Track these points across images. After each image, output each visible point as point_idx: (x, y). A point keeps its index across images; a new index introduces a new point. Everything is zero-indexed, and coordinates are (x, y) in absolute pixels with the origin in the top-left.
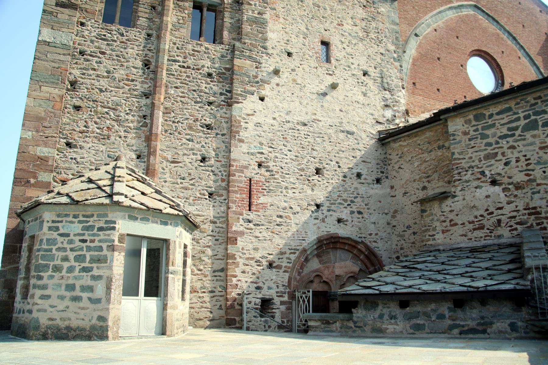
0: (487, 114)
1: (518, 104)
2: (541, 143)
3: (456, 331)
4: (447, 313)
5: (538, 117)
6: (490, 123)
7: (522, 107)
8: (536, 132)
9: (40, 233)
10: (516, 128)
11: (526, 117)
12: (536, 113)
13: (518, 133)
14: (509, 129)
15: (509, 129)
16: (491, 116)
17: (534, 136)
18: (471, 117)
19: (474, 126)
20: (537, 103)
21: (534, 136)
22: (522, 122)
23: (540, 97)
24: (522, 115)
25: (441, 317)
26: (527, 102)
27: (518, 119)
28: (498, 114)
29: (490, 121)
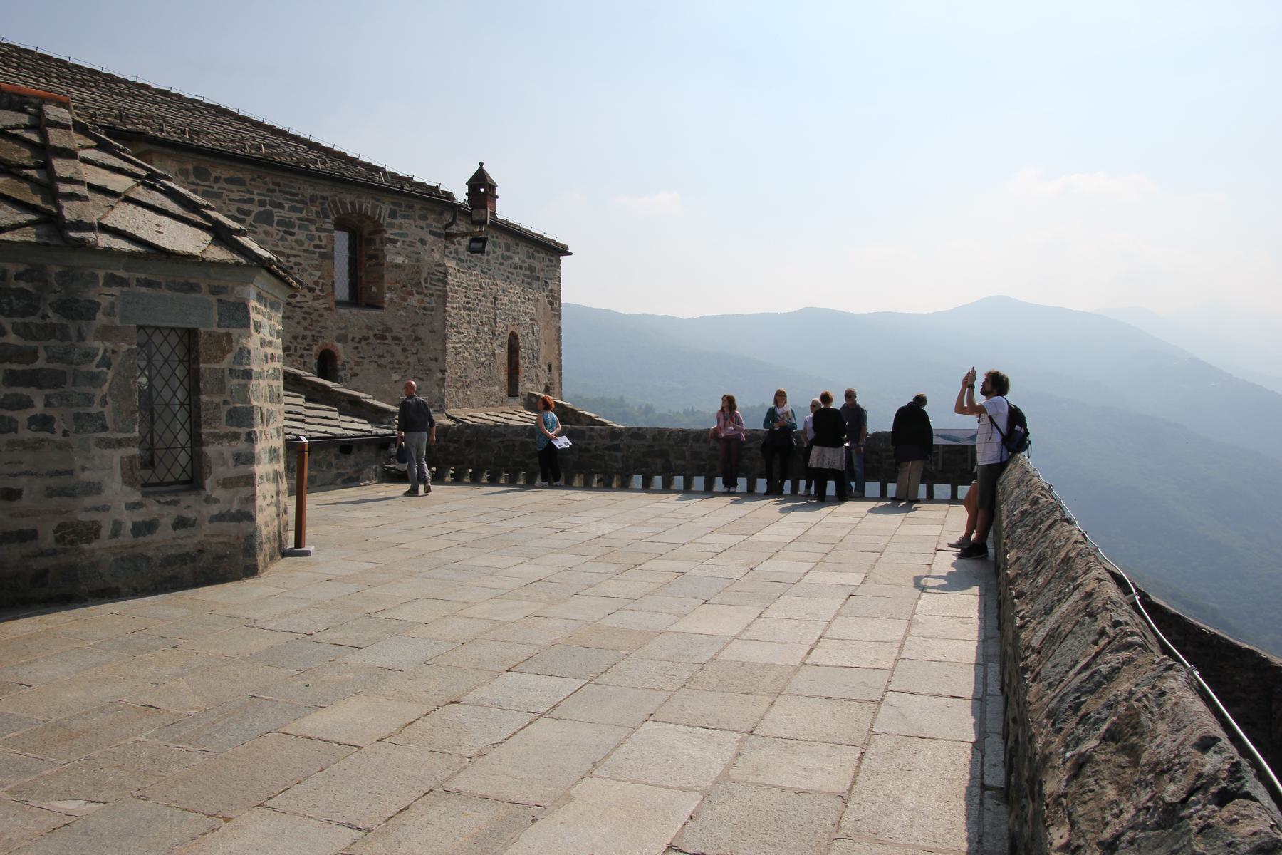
0: (214, 175)
1: (253, 179)
2: (274, 245)
3: (339, 481)
4: (333, 460)
5: (275, 210)
6: (216, 190)
7: (258, 188)
8: (269, 228)
9: (235, 332)
10: (248, 213)
11: (262, 204)
12: (272, 204)
13: (250, 220)
14: (239, 210)
15: (239, 210)
16: (217, 180)
17: (266, 233)
18: (190, 167)
19: (193, 183)
20: (274, 191)
21: (266, 233)
22: (256, 209)
23: (278, 184)
24: (257, 198)
25: (330, 466)
26: (265, 183)
27: (251, 201)
28: (227, 181)
29: (216, 186)
